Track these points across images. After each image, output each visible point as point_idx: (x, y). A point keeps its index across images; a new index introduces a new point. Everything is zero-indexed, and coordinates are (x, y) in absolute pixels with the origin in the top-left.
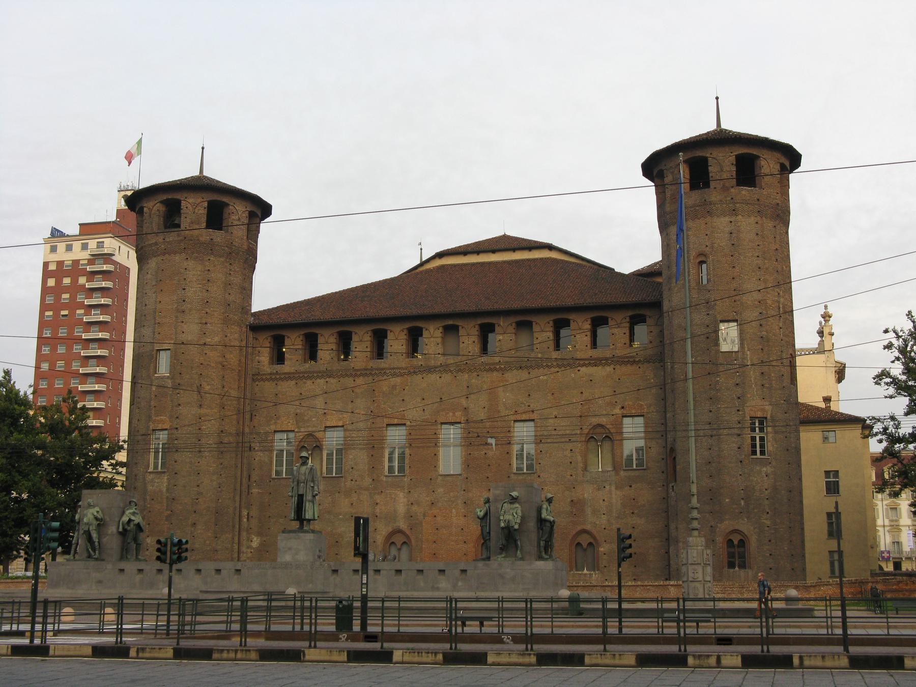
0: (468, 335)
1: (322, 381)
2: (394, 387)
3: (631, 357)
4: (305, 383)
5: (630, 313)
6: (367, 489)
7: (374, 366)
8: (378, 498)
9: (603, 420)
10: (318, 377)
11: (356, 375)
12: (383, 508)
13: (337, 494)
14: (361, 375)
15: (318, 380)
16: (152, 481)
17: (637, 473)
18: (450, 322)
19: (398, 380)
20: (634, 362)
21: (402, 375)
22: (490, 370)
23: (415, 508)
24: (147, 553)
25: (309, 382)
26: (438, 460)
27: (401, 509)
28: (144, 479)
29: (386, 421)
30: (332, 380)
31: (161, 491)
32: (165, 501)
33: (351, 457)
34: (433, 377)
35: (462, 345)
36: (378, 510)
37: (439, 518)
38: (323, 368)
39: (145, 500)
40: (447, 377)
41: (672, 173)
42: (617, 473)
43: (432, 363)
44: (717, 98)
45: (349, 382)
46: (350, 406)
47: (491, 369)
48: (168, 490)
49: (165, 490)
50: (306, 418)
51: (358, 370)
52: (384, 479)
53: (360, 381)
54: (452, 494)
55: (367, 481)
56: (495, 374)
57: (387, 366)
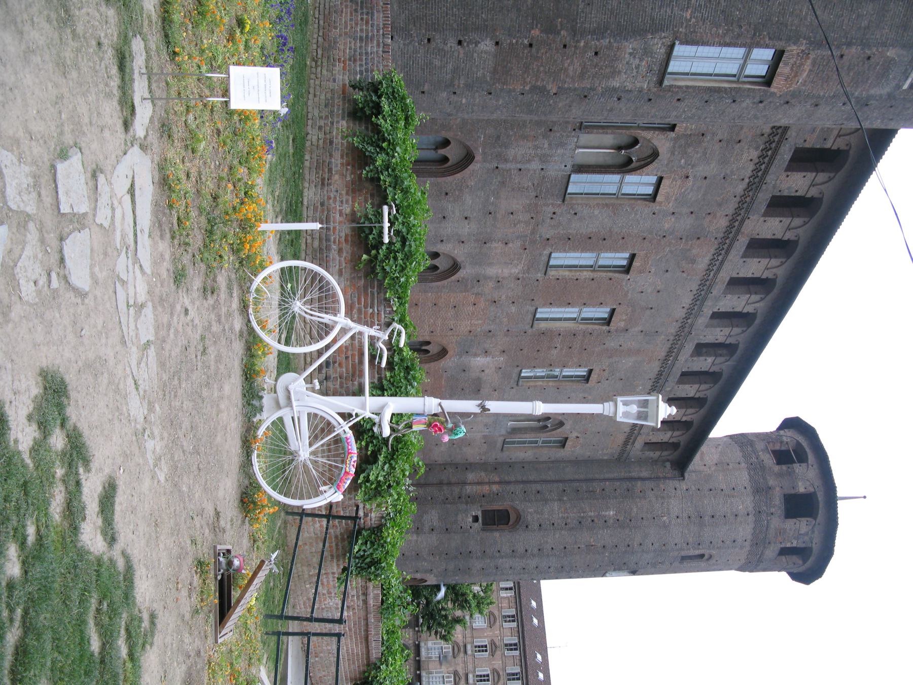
0: (730, 336)
1: (749, 173)
2: (693, 261)
3: (633, 443)
4: (757, 148)
5: (682, 444)
6: (533, 233)
7: (737, 244)
8: (515, 246)
9: (567, 427)
10: (756, 170)
11: (733, 220)
12: (498, 251)
13: (534, 194)
14: (731, 226)
15: (751, 167)
16: (647, 52)
17: (499, 445)
18: (758, 321)
19: (702, 264)
20: (626, 443)
21: (709, 270)
22: (670, 352)
23: (491, 284)
24: (452, 43)
25: (755, 154)
26: (560, 306)
27: (492, 271)
28: (656, 28)
29: (640, 254)
30: (741, 187)
31: (615, 73)
32: (587, 84)
33: (596, 212)
34: (687, 301)
35: (718, 329)
36: (494, 245)
37: (471, 308)
38: (769, 179)
39: (599, 32)
40: (680, 314)
41: (807, 534)
42: (500, 436)
43: (709, 303)
44: (865, 497)
45: (730, 208)
46: (685, 210)
47: (672, 352)
48: (615, 89)
49: (616, 83)
50: (689, 150)
51: (742, 221)
52: (546, 252)
53: (723, 223)
54: (505, 320)
55: (546, 231)
56: (664, 354)
57: (730, 257)
